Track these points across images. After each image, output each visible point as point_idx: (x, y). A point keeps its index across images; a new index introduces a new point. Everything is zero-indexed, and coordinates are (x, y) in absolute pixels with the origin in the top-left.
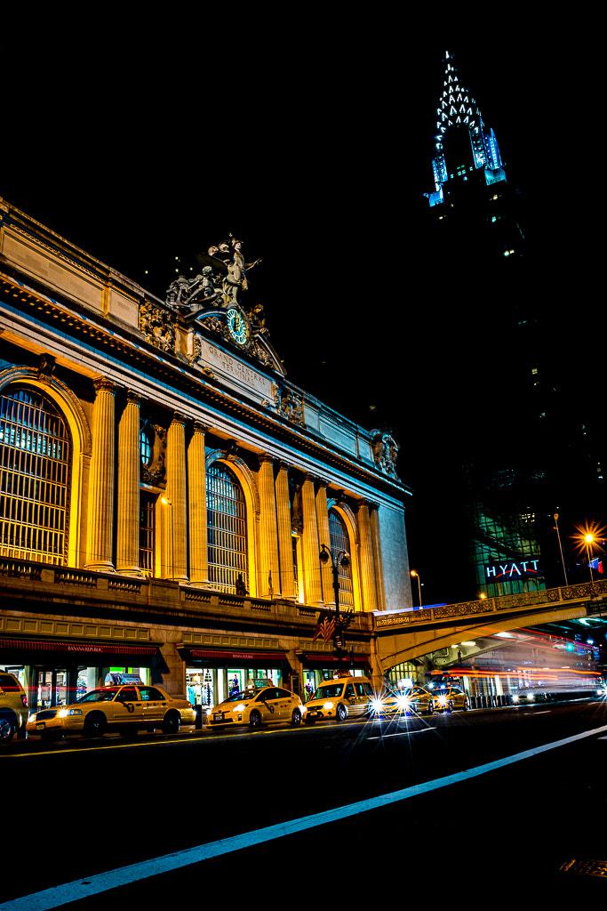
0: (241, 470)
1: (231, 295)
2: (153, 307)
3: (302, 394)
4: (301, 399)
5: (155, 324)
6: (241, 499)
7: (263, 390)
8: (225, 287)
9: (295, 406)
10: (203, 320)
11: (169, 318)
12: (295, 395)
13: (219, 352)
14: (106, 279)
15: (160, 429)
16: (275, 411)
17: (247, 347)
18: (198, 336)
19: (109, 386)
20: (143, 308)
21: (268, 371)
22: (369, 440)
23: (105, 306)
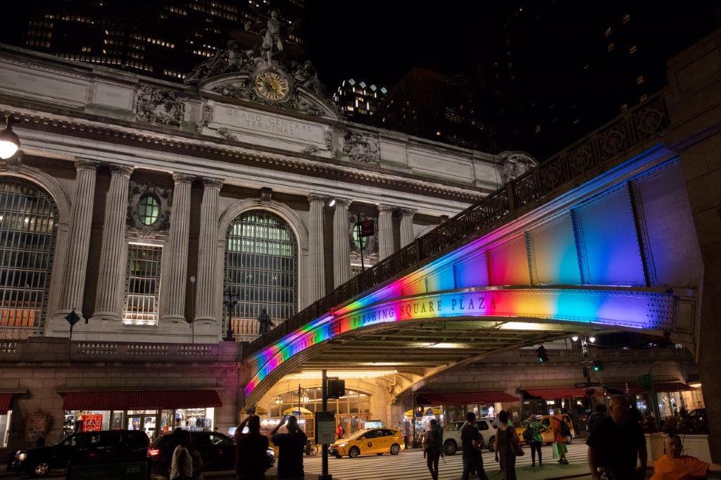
0: (284, 211)
1: (266, 60)
2: (154, 89)
3: (378, 133)
4: (377, 137)
5: (157, 103)
6: (293, 242)
7: (309, 136)
8: (262, 53)
9: (365, 145)
10: (215, 89)
11: (171, 94)
12: (368, 135)
13: (241, 113)
14: (93, 76)
15: (162, 191)
16: (328, 155)
17: (287, 100)
18: (210, 103)
19: (88, 165)
20: (140, 92)
21: (314, 117)
22: (493, 162)
23: (90, 99)
